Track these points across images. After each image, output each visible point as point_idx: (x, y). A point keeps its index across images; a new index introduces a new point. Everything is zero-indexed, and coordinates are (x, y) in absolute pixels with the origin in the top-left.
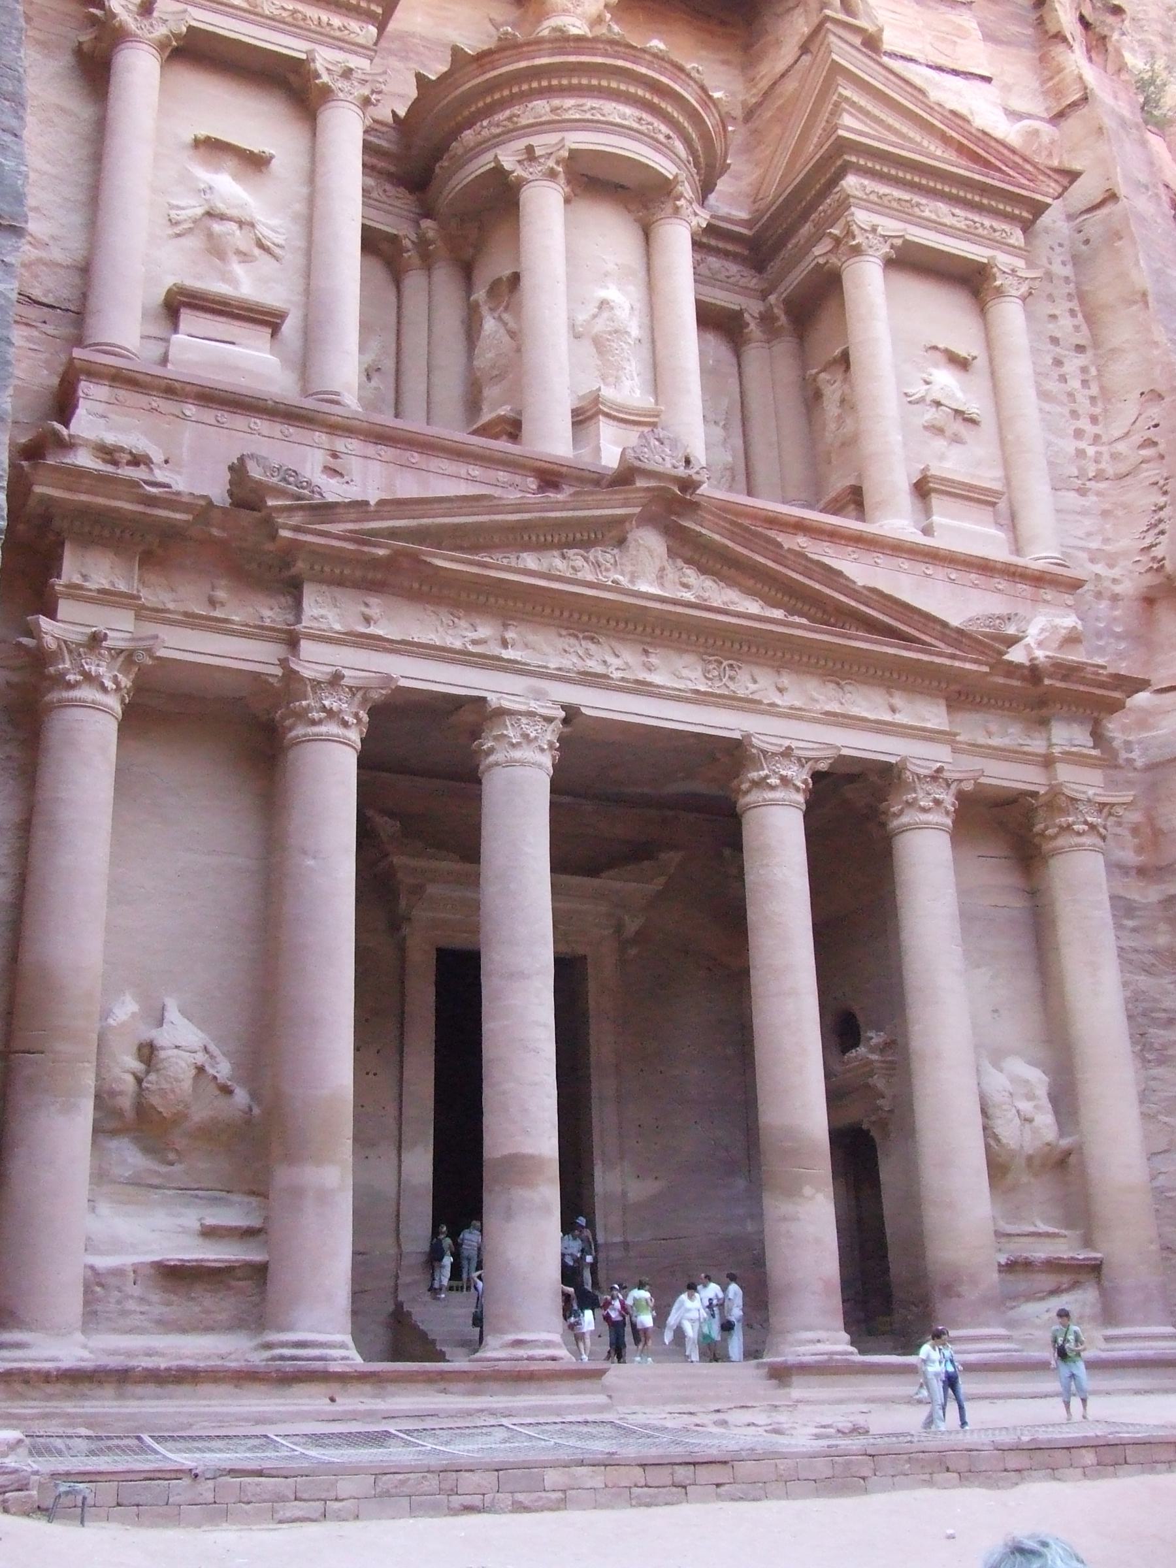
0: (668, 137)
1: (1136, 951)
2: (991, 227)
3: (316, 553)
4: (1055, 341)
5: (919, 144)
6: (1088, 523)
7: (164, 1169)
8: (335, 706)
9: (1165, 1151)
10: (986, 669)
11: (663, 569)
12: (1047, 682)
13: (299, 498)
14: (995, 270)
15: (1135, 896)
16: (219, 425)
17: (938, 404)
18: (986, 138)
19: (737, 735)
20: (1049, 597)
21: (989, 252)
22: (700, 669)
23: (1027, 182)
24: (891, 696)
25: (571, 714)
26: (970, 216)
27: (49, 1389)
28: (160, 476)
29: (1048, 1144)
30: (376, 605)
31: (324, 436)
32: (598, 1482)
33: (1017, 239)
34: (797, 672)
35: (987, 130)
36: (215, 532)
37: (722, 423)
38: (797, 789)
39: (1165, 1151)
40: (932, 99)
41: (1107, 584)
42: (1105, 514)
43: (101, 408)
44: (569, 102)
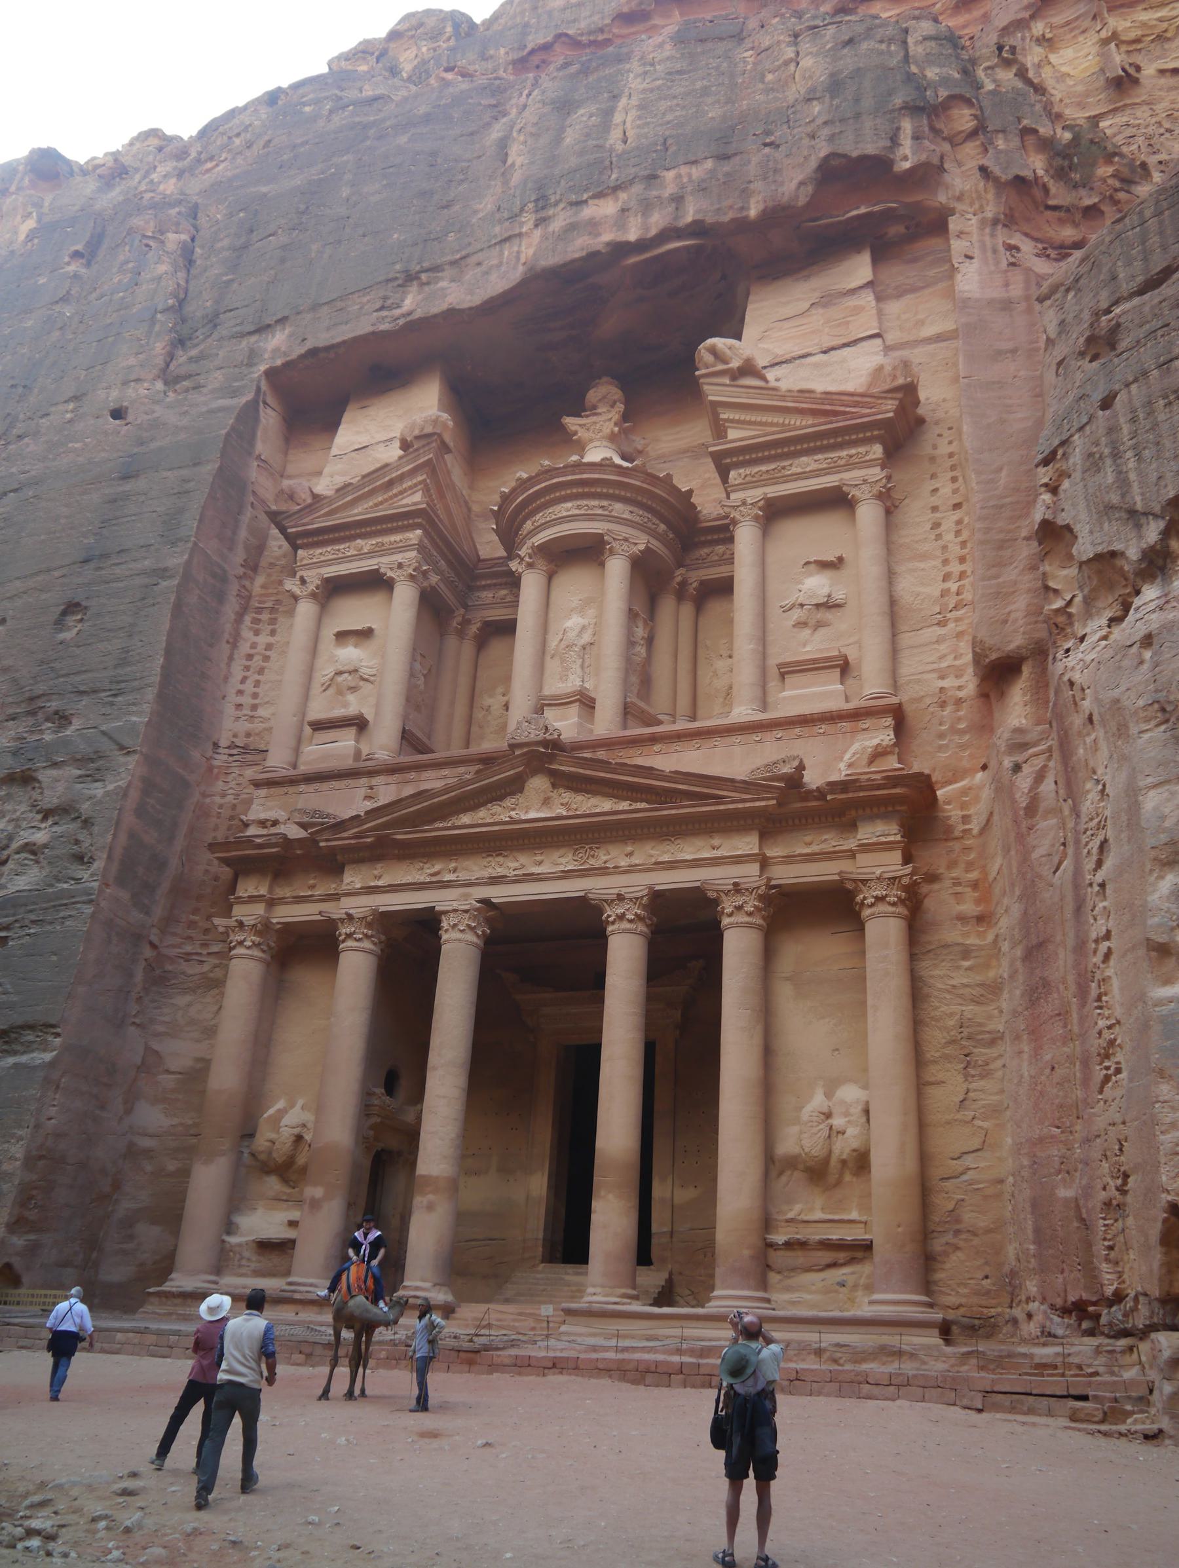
1: (967, 986)
4: (935, 509)
5: (783, 425)
6: (943, 648)
7: (289, 1190)
8: (348, 931)
10: (774, 802)
11: (549, 798)
12: (829, 797)
13: (323, 824)
14: (845, 488)
15: (972, 940)
16: (316, 791)
17: (802, 605)
19: (582, 894)
20: (866, 726)
21: (836, 477)
22: (571, 855)
23: (868, 411)
25: (486, 902)
26: (826, 456)
27: (178, 1301)
29: (854, 1150)
30: (379, 868)
31: (365, 780)
32: (136, 1341)
34: (641, 840)
36: (299, 852)
38: (631, 921)
41: (950, 693)
42: (959, 635)
44: (537, 517)
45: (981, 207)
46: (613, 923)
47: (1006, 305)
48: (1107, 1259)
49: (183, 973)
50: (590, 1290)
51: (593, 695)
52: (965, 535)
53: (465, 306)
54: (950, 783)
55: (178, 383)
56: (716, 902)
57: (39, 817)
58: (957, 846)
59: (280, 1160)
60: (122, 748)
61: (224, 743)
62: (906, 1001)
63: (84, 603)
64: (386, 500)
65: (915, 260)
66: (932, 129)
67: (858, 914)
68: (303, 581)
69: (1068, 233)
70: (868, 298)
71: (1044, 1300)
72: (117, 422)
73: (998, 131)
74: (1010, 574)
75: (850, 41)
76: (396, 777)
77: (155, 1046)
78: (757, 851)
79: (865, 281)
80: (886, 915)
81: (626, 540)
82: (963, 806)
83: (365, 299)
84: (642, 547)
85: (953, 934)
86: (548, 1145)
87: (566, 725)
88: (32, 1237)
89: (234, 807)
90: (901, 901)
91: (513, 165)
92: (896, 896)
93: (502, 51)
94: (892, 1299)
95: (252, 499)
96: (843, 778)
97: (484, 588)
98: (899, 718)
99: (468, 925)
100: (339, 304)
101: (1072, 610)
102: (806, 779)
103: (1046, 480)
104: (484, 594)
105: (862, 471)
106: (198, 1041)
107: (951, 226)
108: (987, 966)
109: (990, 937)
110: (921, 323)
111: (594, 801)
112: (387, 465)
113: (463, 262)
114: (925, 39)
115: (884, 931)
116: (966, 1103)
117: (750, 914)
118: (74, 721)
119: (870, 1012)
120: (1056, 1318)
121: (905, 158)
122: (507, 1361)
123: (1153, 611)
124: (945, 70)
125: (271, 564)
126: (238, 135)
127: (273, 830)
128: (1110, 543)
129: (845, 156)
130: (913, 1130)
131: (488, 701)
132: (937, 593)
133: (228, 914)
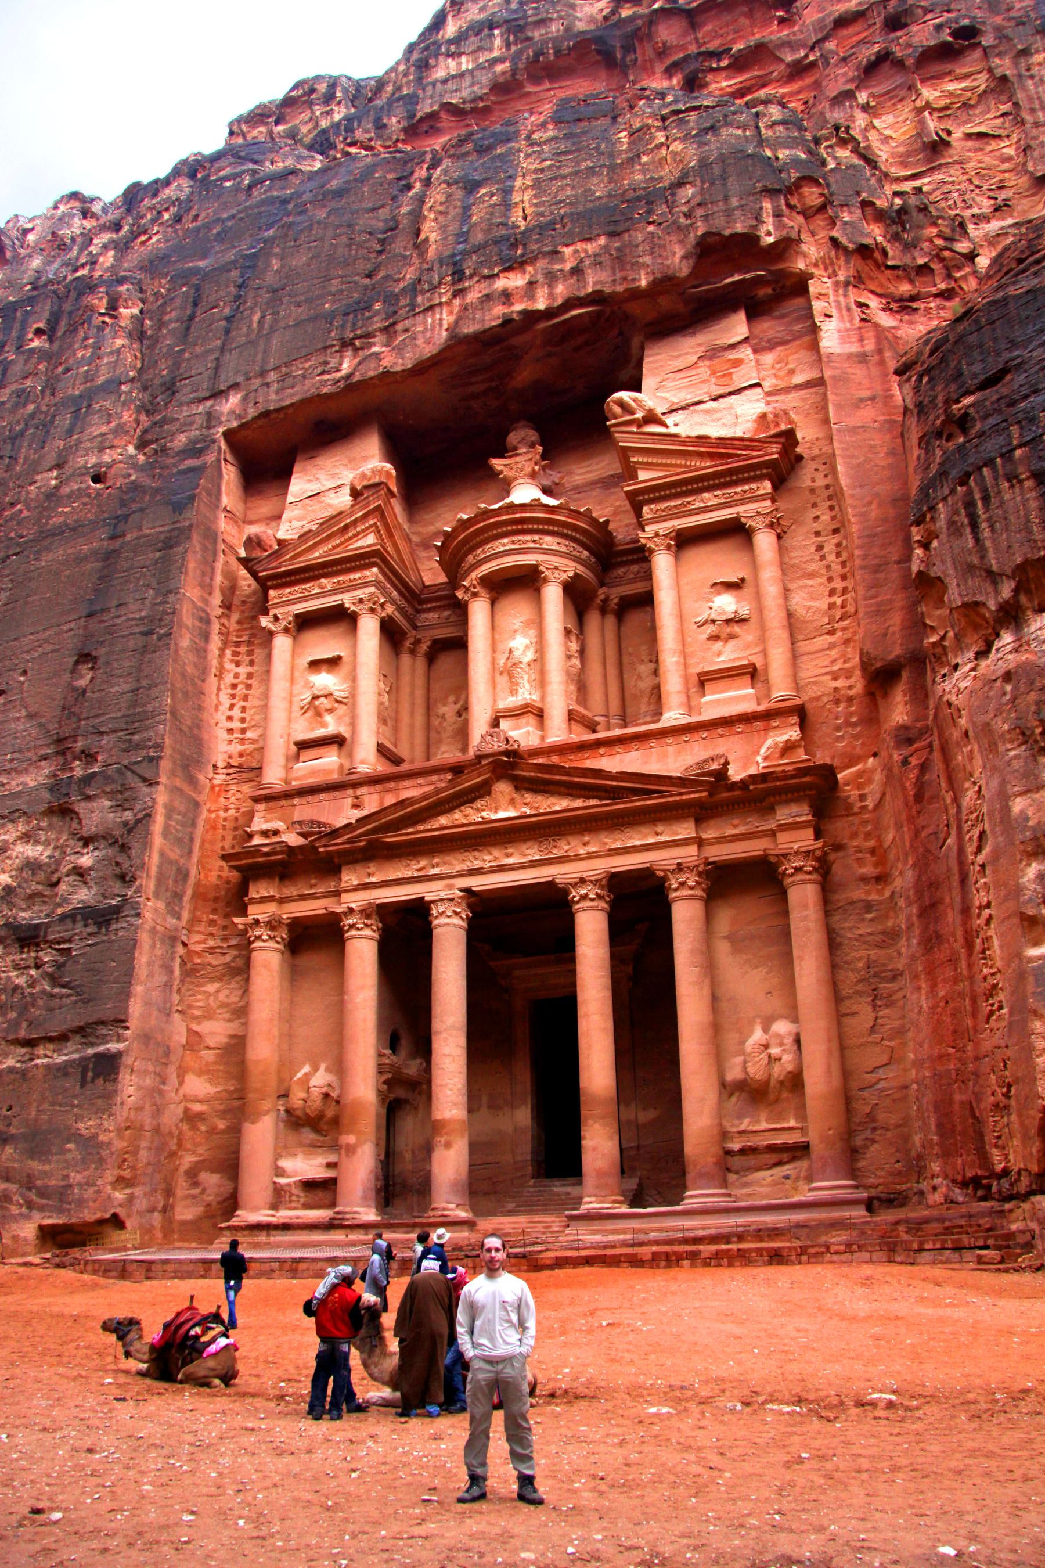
0: (534, 541)
3: (338, 852)
4: (817, 534)
5: (686, 466)
6: (833, 653)
10: (705, 794)
14: (743, 520)
15: (873, 897)
16: (308, 803)
17: (713, 621)
25: (467, 890)
28: (284, 838)
30: (372, 867)
38: (592, 900)
40: (683, 435)
42: (847, 642)
43: (262, 814)
45: (834, 271)
46: (578, 902)
47: (862, 358)
48: (996, 1146)
49: (210, 965)
50: (586, 1199)
51: (540, 705)
52: (844, 556)
53: (399, 368)
55: (145, 447)
56: (664, 879)
57: (81, 844)
58: (856, 820)
59: (312, 1115)
60: (145, 780)
61: (220, 764)
62: (825, 951)
63: (94, 654)
64: (342, 543)
65: (782, 317)
66: (789, 206)
67: (780, 883)
68: (276, 618)
69: (905, 288)
70: (746, 353)
71: (946, 1177)
72: (98, 486)
73: (842, 206)
74: (885, 595)
75: (712, 128)
76: (379, 787)
77: (195, 1027)
79: (742, 337)
80: (804, 882)
81: (556, 568)
82: (860, 786)
83: (307, 365)
84: (571, 574)
85: (858, 893)
86: (528, 1085)
87: (523, 735)
88: (128, 1191)
89: (236, 819)
90: (815, 870)
91: (427, 239)
93: (394, 120)
94: (830, 1186)
95: (223, 547)
96: (762, 771)
97: (429, 610)
98: (801, 714)
99: (456, 913)
100: (284, 369)
101: (946, 643)
102: (730, 772)
103: (918, 538)
104: (430, 615)
105: (752, 505)
106: (229, 1020)
107: (811, 289)
108: (887, 917)
109: (887, 894)
110: (792, 372)
111: (553, 800)
112: (341, 513)
113: (391, 330)
114: (775, 124)
115: (803, 897)
117: (692, 888)
118: (100, 758)
119: (796, 962)
120: (957, 1191)
121: (769, 234)
122: (548, 1262)
123: (1010, 652)
124: (793, 152)
125: (244, 602)
126: (167, 210)
127: (275, 839)
128: (974, 594)
129: (719, 234)
130: (836, 1054)
131: (442, 710)
132: (825, 607)
133: (244, 913)
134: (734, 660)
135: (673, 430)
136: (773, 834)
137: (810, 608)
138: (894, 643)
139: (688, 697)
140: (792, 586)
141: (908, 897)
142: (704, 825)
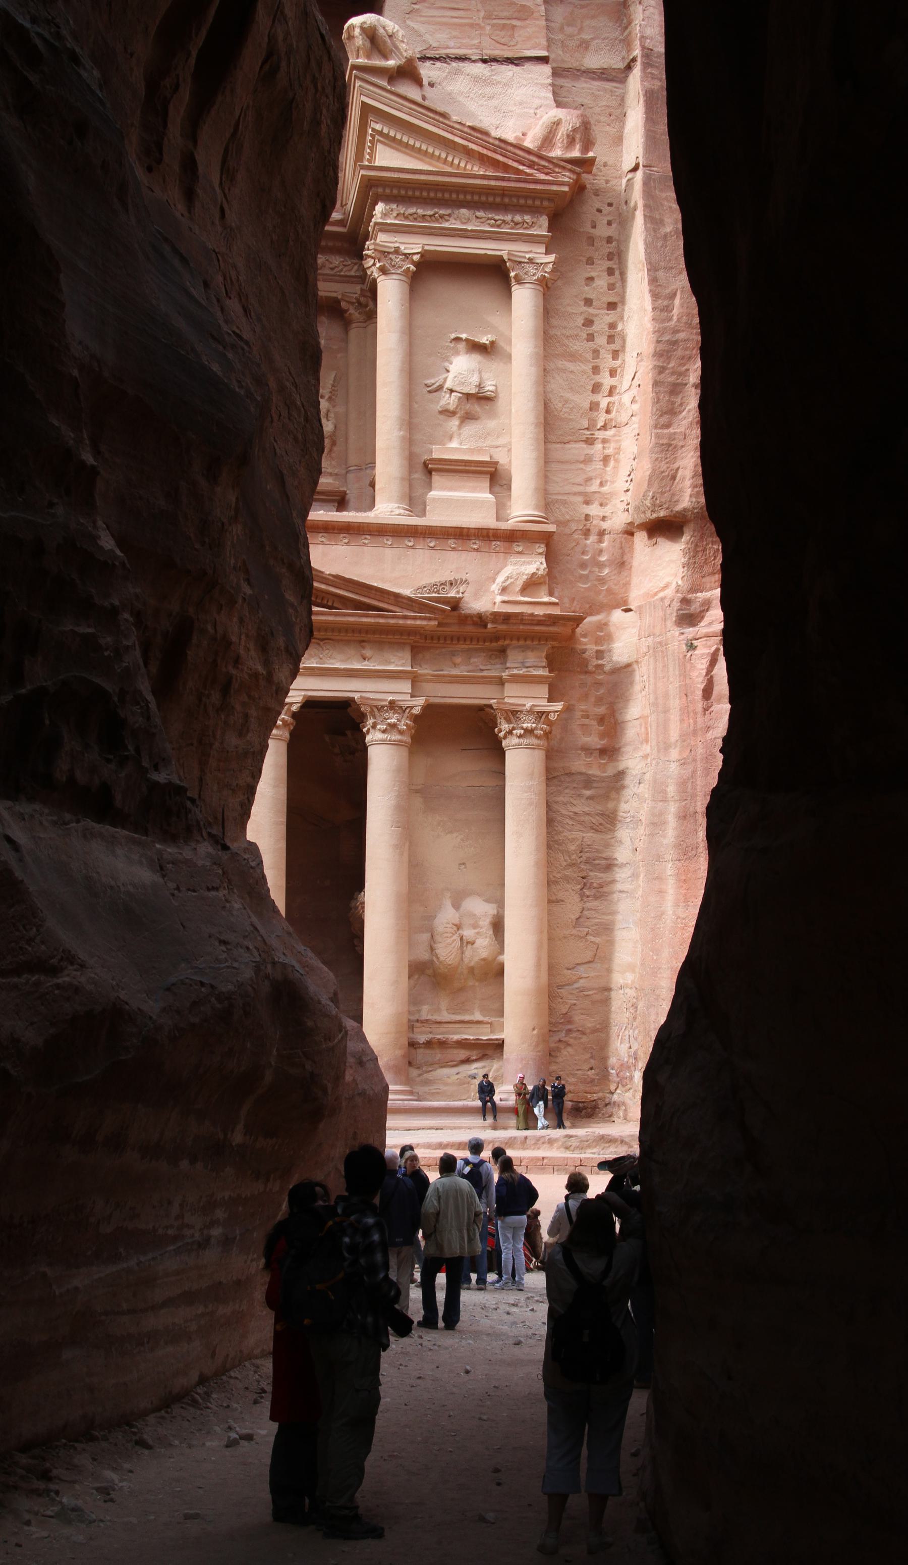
1: (588, 814)
2: (512, 221)
4: (588, 302)
9: (589, 962)
10: (435, 623)
15: (594, 771)
17: (452, 391)
18: (503, 145)
20: (520, 549)
24: (363, 647)
29: (484, 960)
33: (540, 227)
35: (504, 137)
37: (327, 397)
39: (589, 962)
40: (454, 118)
54: (591, 615)
58: (589, 679)
78: (410, 669)
82: (598, 641)
85: (580, 764)
90: (545, 732)
92: (542, 729)
108: (606, 797)
109: (610, 771)
110: (585, 45)
116: (581, 920)
117: (401, 732)
134: (471, 451)
135: (434, 98)
136: (501, 682)
137: (566, 401)
138: (682, 490)
139: (411, 486)
140: (552, 366)
141: (666, 793)
142: (421, 656)
